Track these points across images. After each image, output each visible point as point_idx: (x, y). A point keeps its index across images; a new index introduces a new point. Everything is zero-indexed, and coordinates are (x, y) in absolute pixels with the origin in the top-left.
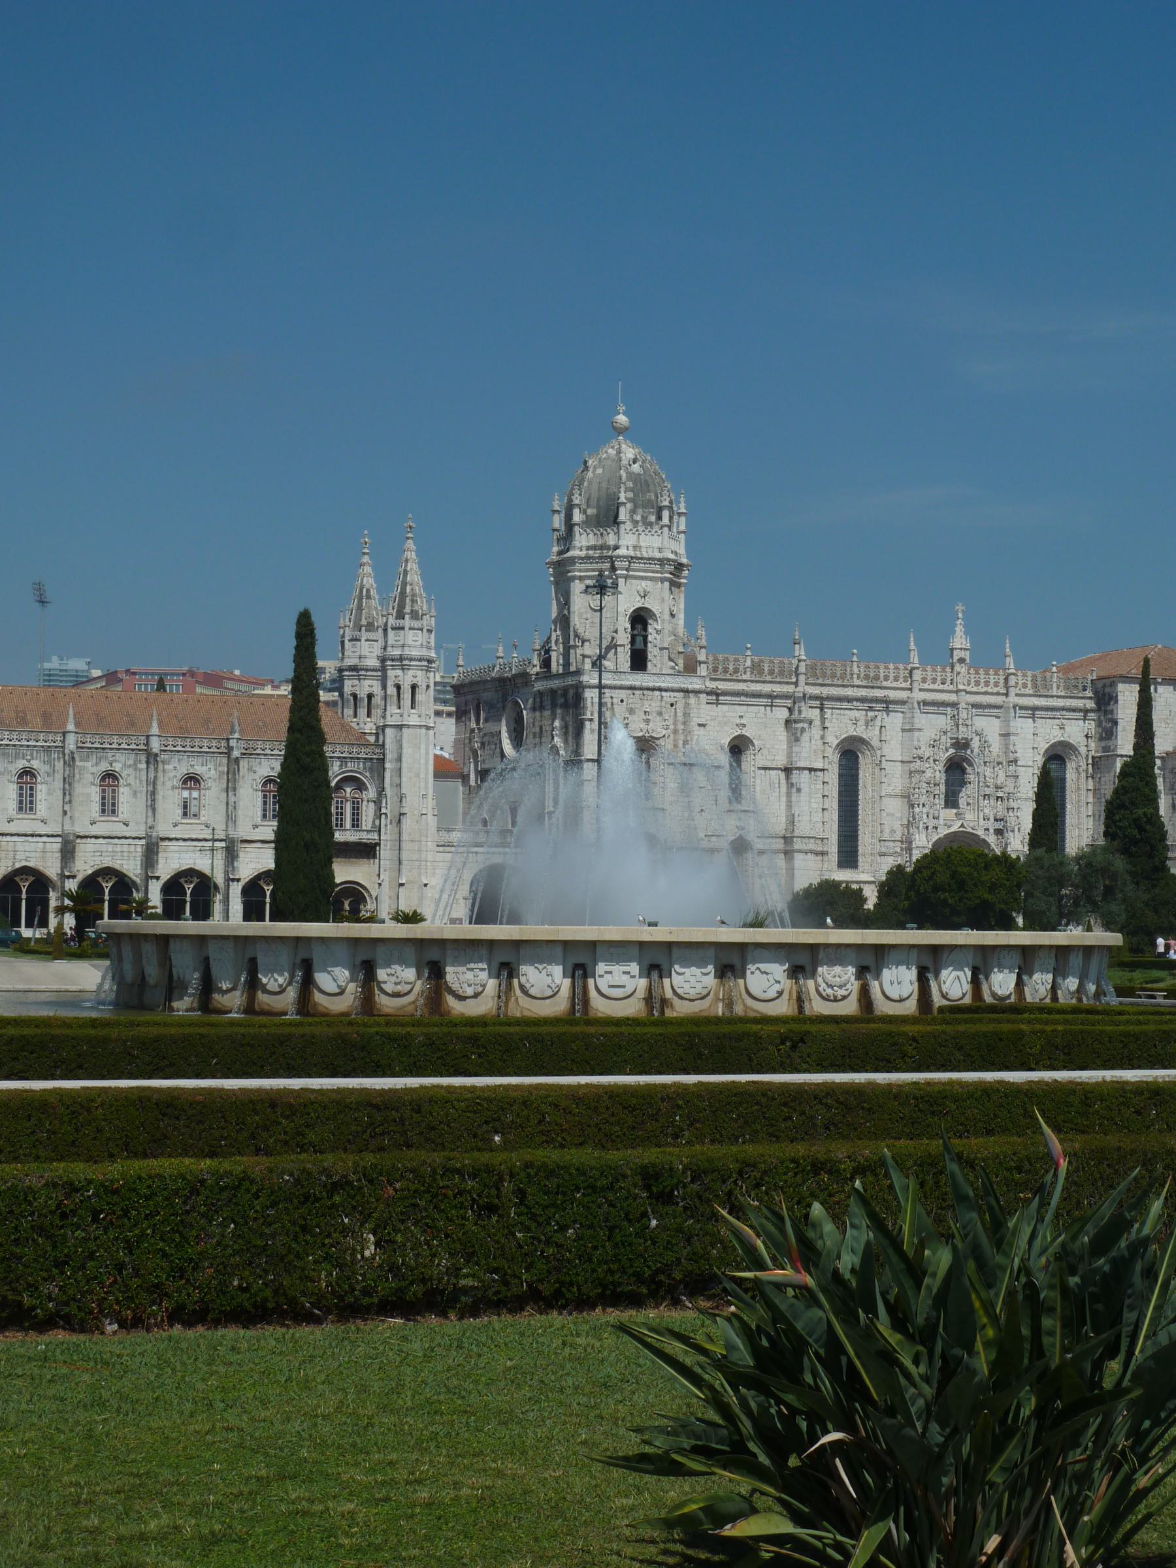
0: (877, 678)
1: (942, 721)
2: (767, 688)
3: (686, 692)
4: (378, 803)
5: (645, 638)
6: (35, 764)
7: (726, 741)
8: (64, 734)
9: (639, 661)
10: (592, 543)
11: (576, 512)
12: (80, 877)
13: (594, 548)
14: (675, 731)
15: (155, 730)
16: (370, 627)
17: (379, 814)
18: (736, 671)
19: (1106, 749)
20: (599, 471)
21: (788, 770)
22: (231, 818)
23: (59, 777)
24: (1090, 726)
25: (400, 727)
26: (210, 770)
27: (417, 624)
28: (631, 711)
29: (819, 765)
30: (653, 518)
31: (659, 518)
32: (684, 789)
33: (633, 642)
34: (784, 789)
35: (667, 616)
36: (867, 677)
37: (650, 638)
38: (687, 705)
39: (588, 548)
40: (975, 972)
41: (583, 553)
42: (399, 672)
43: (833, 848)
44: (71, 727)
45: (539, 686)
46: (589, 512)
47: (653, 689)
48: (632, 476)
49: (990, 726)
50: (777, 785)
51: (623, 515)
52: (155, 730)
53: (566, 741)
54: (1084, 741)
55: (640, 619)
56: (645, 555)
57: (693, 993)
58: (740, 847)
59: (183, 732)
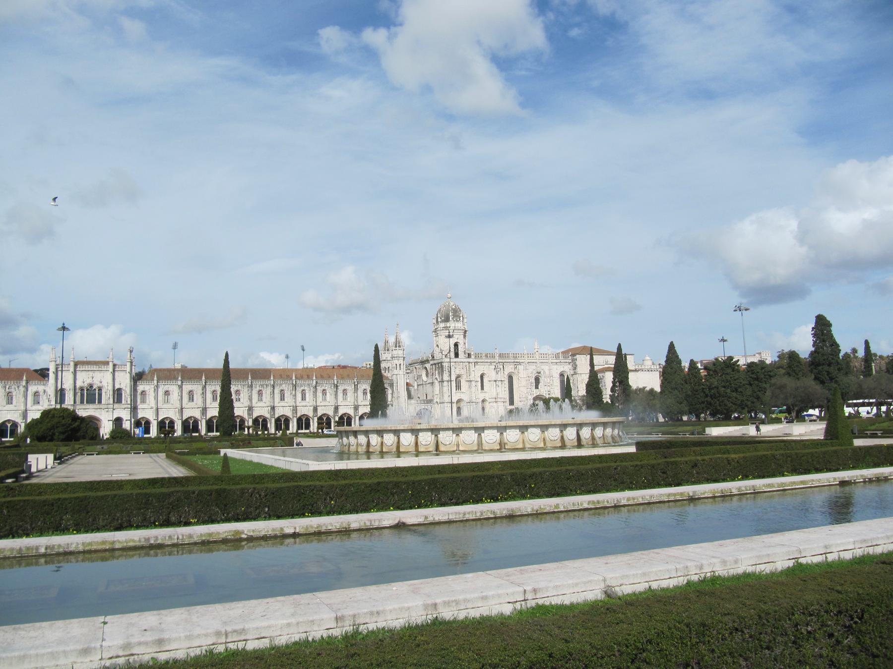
0: (516, 357)
1: (534, 367)
2: (489, 361)
3: (469, 363)
4: (392, 394)
5: (458, 349)
6: (306, 388)
8: (313, 380)
9: (457, 355)
11: (439, 318)
12: (318, 416)
13: (444, 327)
14: (467, 372)
15: (335, 378)
16: (388, 350)
17: (392, 397)
18: (481, 357)
19: (575, 372)
20: (444, 308)
21: (495, 381)
22: (356, 399)
23: (312, 391)
24: (570, 366)
25: (397, 375)
26: (350, 388)
27: (400, 348)
28: (455, 368)
29: (503, 380)
32: (470, 387)
33: (455, 351)
34: (495, 386)
35: (463, 344)
36: (514, 357)
37: (459, 349)
38: (469, 366)
40: (592, 429)
42: (397, 361)
43: (508, 402)
44: (314, 378)
45: (432, 362)
48: (452, 309)
49: (546, 368)
51: (451, 319)
52: (335, 378)
53: (439, 376)
54: (568, 370)
55: (456, 345)
57: (513, 441)
58: (483, 401)
59: (342, 378)
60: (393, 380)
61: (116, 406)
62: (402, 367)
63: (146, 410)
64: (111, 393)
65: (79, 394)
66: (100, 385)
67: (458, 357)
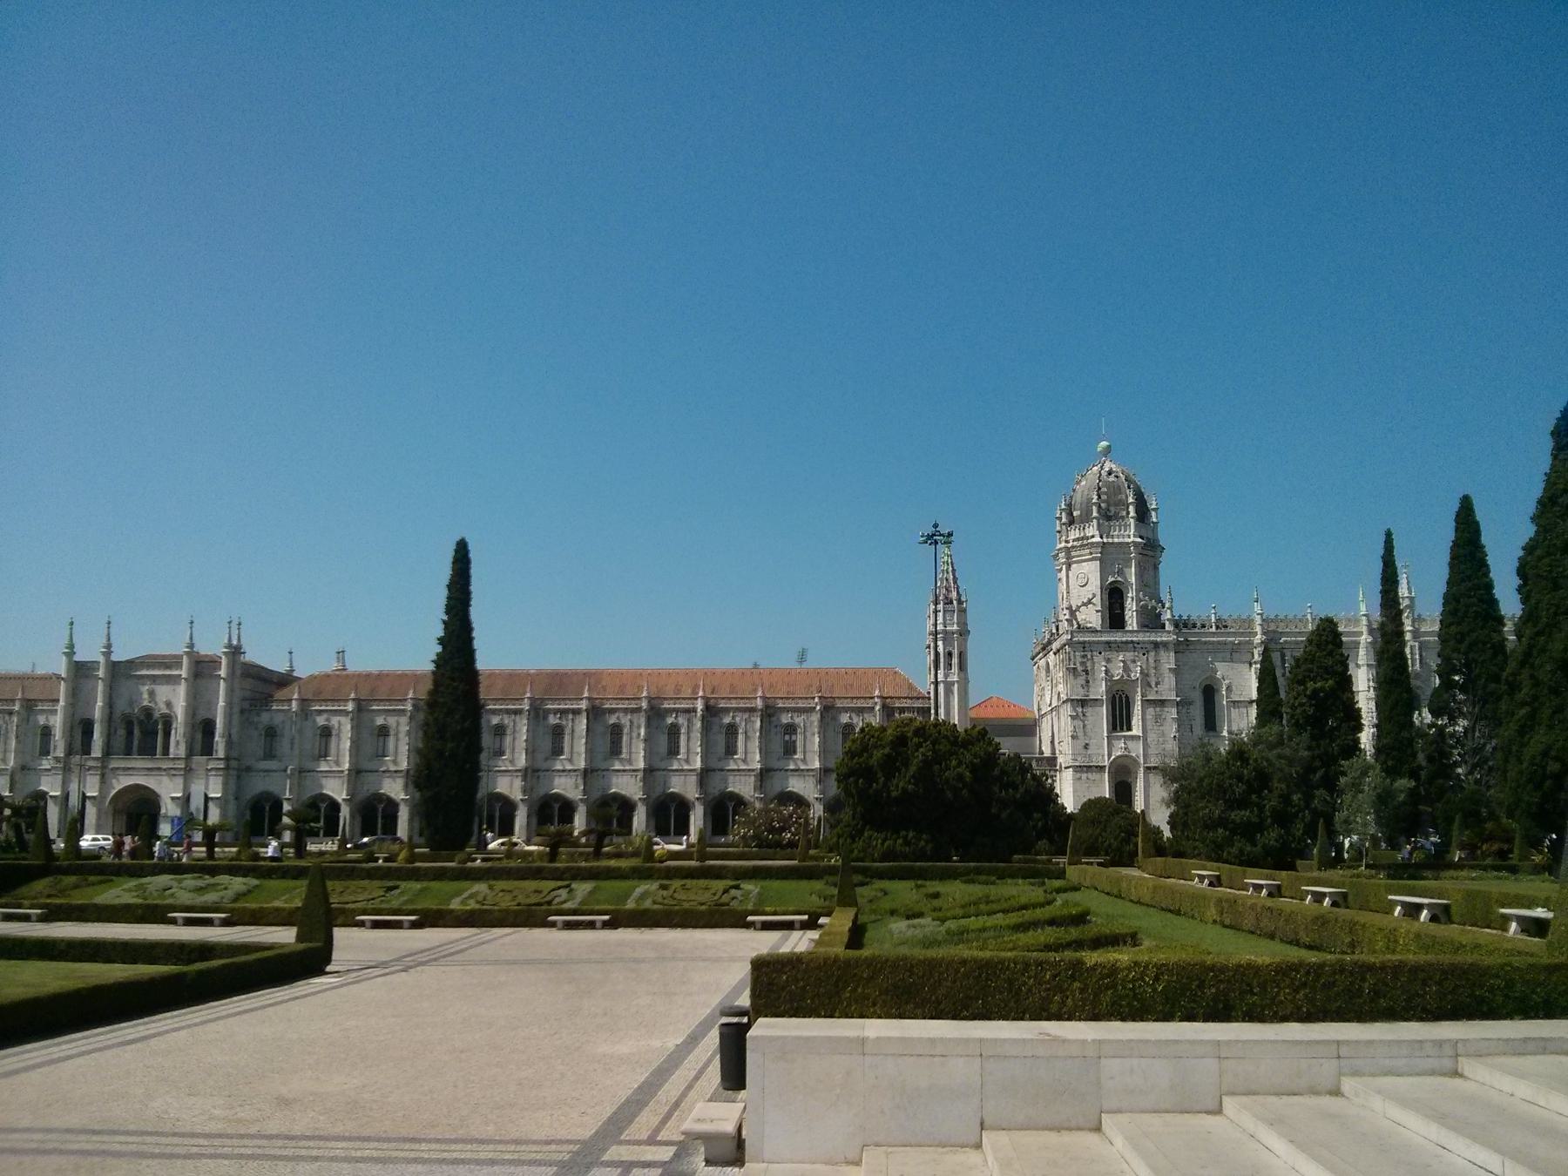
3: (1156, 645)
7: (1195, 681)
9: (1115, 619)
10: (1077, 536)
13: (1078, 539)
15: (760, 694)
20: (1083, 483)
27: (949, 607)
28: (1108, 661)
30: (1124, 513)
31: (1128, 513)
39: (1074, 541)
41: (1069, 545)
45: (1055, 646)
46: (1075, 514)
47: (1127, 642)
50: (1245, 715)
56: (1116, 540)
60: (929, 698)
61: (199, 760)
62: (955, 660)
63: (271, 774)
64: (181, 730)
65: (122, 732)
66: (165, 710)
67: (1124, 628)
